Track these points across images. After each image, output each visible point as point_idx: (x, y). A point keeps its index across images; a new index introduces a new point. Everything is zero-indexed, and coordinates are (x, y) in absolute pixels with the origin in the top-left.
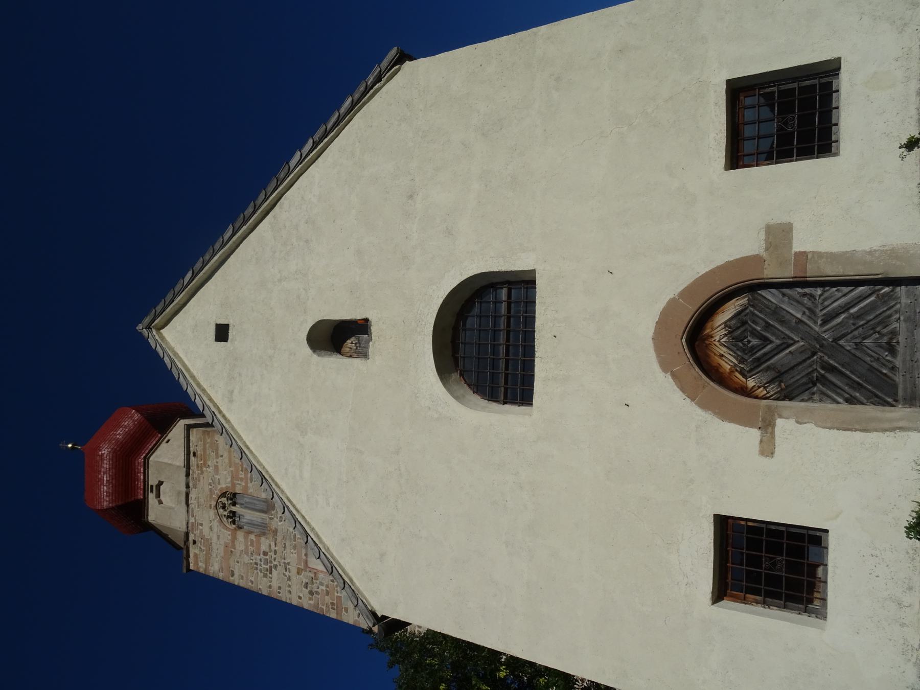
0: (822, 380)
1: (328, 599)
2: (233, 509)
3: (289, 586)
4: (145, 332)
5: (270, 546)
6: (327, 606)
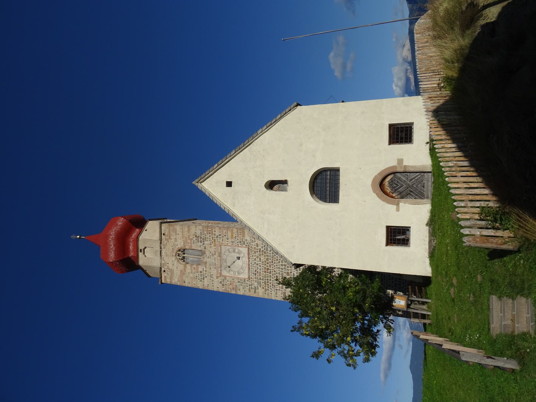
0: (409, 194)
2: (184, 256)
4: (196, 184)
6: (231, 289)
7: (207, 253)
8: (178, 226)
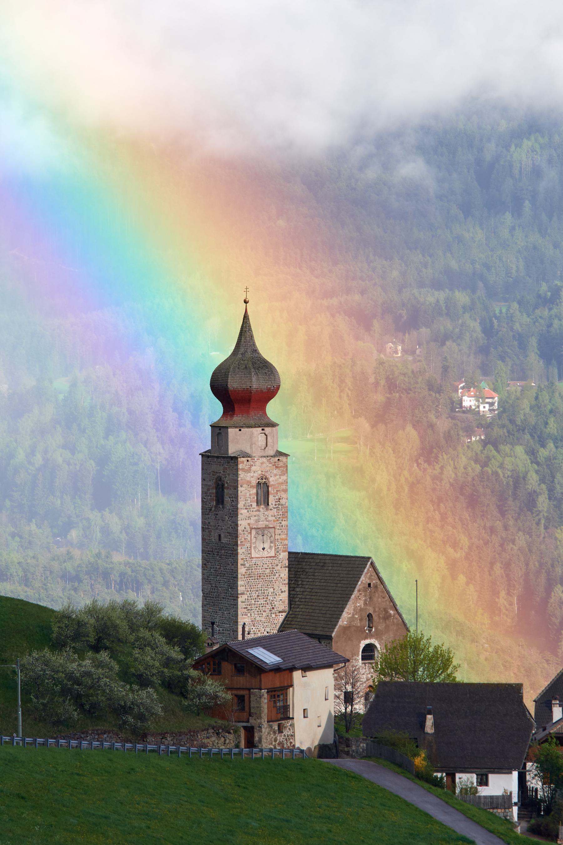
1: (243, 540)
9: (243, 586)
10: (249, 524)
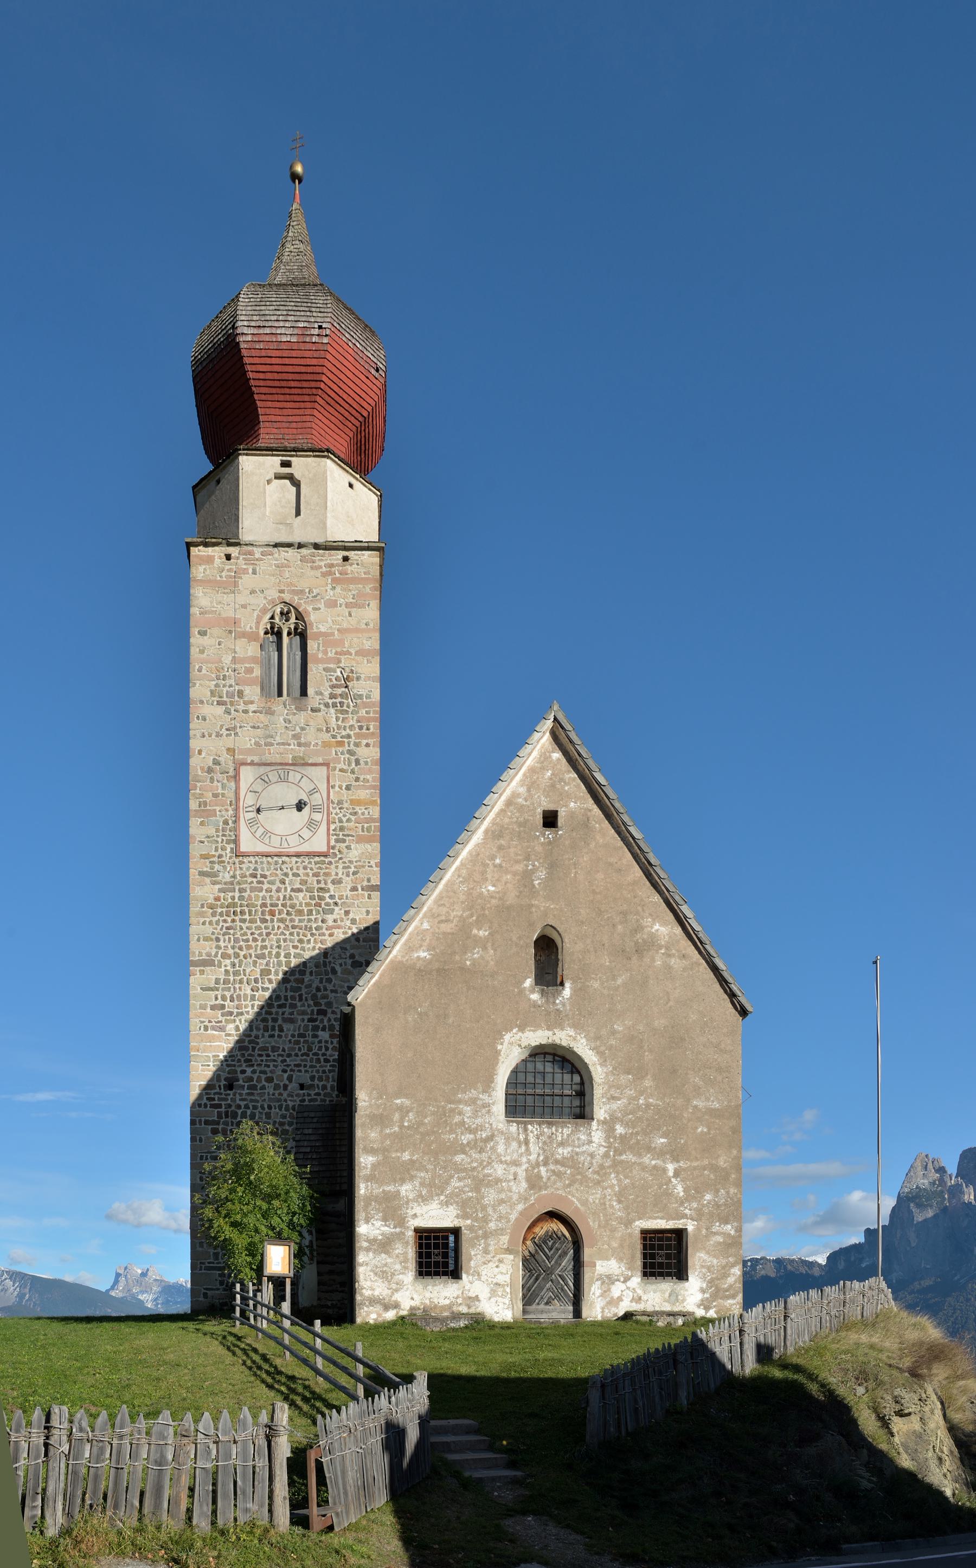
1: (209, 797)
3: (210, 736)
5: (252, 702)
7: (301, 718)
8: (371, 613)
9: (206, 939)
10: (231, 751)
